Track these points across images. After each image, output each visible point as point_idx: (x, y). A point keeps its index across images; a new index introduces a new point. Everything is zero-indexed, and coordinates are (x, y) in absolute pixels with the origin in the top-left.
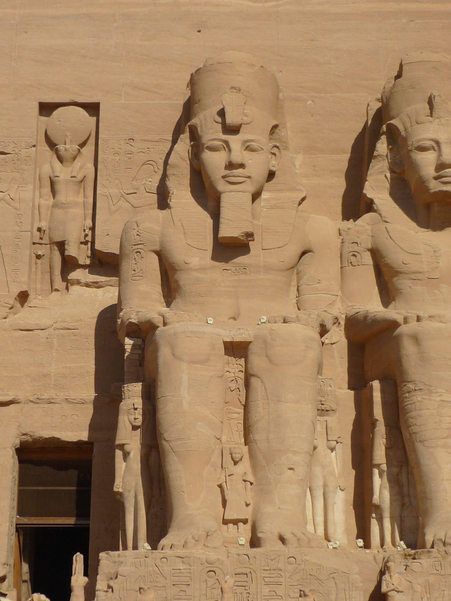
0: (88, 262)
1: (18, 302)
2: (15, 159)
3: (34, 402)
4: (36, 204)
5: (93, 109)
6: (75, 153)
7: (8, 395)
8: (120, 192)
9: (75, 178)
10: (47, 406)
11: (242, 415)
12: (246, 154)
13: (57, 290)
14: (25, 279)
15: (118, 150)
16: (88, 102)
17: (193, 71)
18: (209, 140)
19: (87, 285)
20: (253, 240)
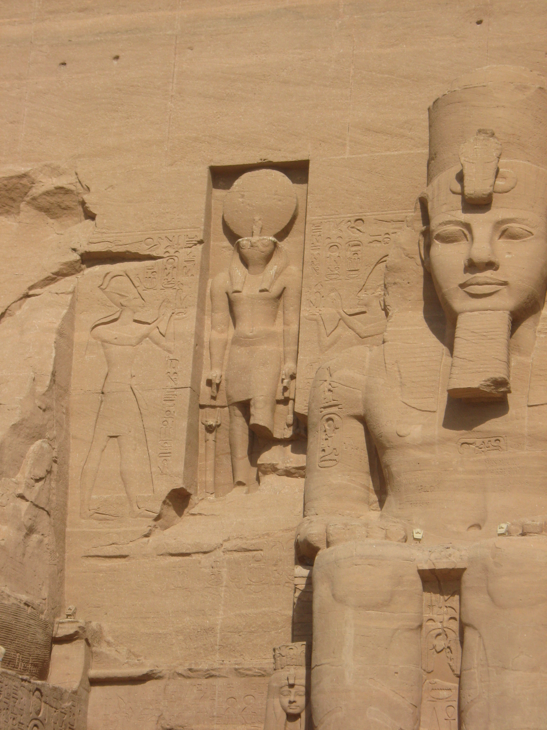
1: (171, 508)
2: (169, 266)
3: (184, 676)
4: (206, 339)
5: (297, 171)
6: (268, 249)
7: (142, 665)
8: (339, 313)
9: (266, 292)
10: (204, 681)
11: (455, 694)
12: (502, 244)
13: (240, 484)
14: (180, 468)
15: (338, 241)
16: (290, 159)
17: (431, 104)
18: (440, 224)
19: (288, 473)
20: (510, 392)
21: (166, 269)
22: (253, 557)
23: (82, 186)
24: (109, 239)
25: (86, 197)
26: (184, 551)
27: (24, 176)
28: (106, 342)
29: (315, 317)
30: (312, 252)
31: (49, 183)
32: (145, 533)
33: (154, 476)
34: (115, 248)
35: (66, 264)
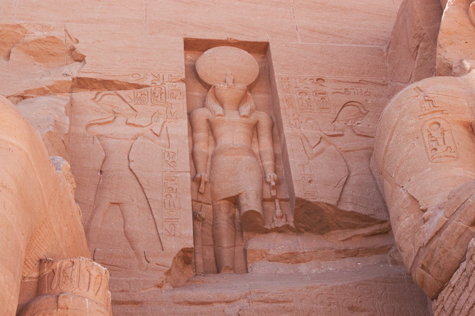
0: (280, 223)
2: (157, 92)
6: (242, 93)
21: (155, 93)
22: (284, 307)
23: (71, 38)
24: (99, 72)
25: (76, 46)
26: (204, 300)
27: (19, 26)
28: (101, 136)
29: (299, 134)
30: (285, 94)
31: (39, 34)
32: (159, 283)
33: (161, 237)
34: (105, 77)
35: (59, 82)
